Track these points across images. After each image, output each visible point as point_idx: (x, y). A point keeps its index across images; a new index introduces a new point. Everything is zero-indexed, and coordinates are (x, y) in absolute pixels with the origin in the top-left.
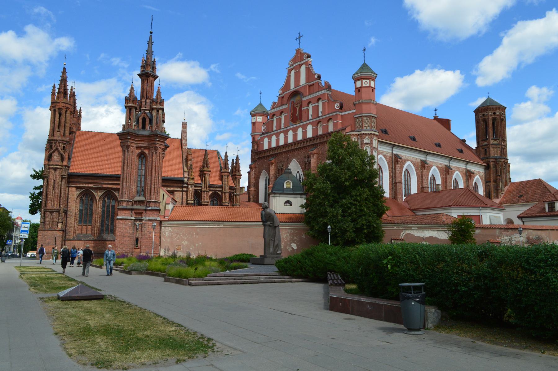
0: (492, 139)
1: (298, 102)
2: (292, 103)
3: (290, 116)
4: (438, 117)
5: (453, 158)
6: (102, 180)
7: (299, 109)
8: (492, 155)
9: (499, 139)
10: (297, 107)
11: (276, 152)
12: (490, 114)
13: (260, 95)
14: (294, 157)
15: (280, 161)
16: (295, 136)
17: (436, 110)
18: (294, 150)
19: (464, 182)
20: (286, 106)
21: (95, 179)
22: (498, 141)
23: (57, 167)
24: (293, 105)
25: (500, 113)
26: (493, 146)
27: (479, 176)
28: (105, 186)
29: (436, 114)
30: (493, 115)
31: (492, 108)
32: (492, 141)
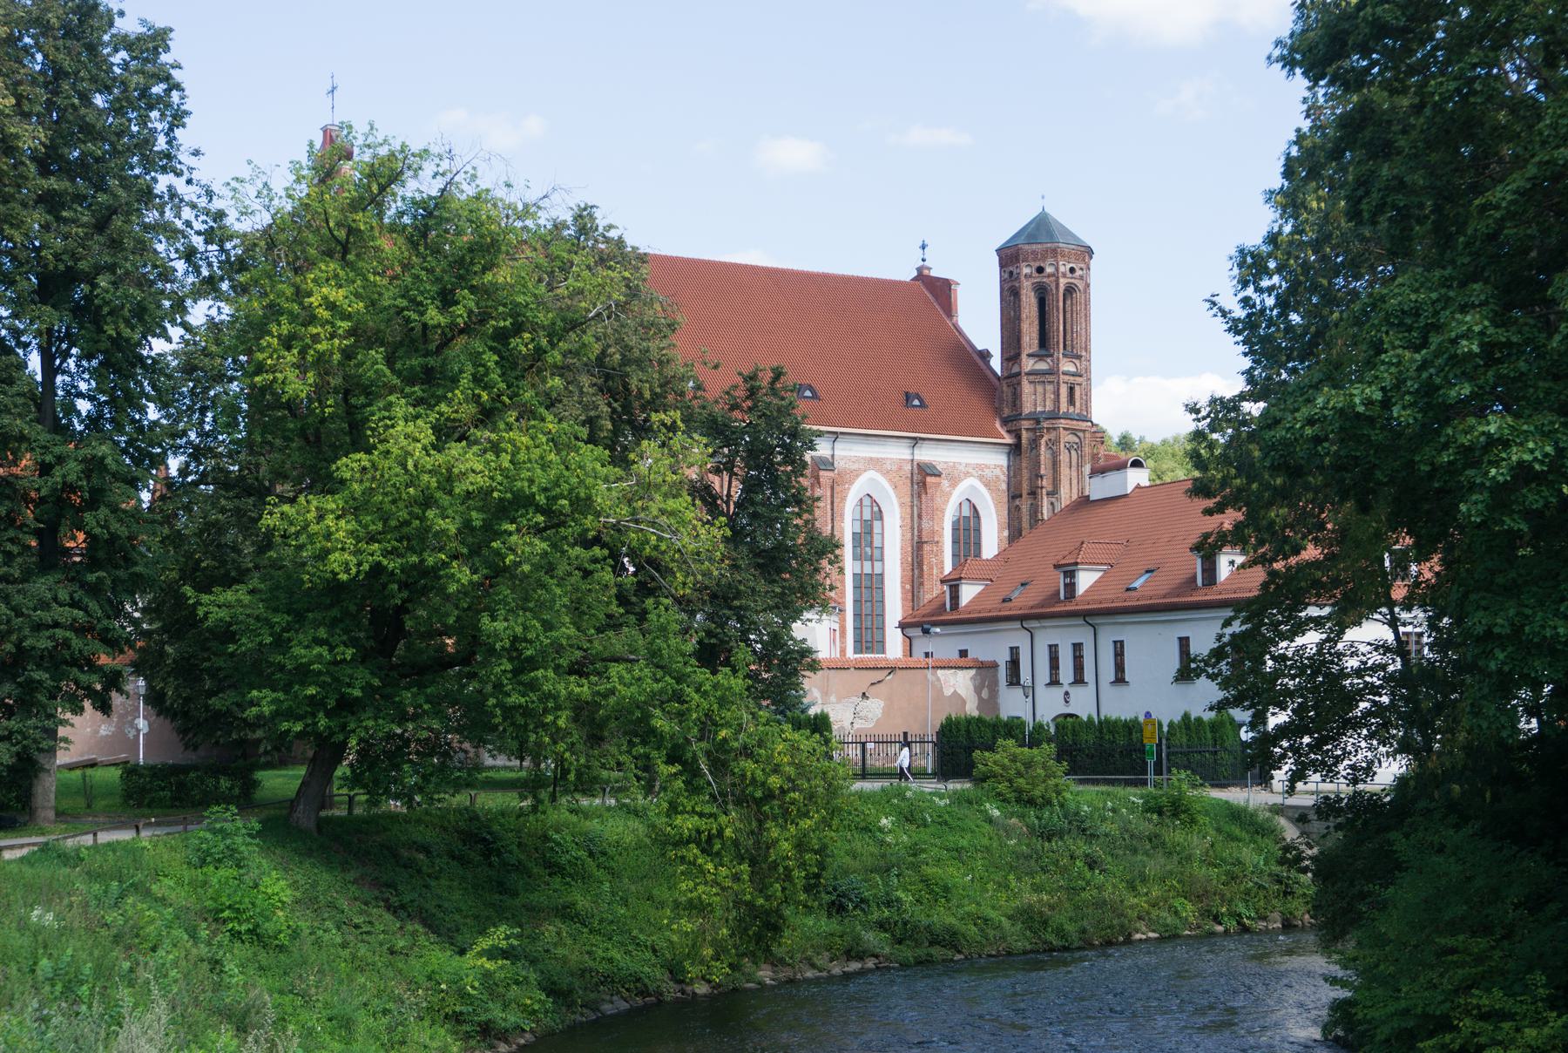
0: (1029, 355)
4: (929, 269)
5: (842, 433)
8: (1027, 408)
9: (1052, 356)
12: (1026, 270)
17: (923, 247)
19: (902, 505)
22: (1049, 360)
25: (1057, 269)
26: (1031, 378)
27: (981, 478)
29: (924, 260)
30: (1035, 274)
31: (1033, 252)
32: (1031, 361)
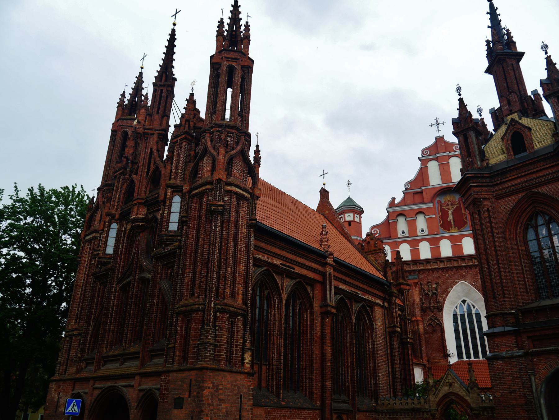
1: (450, 203)
2: (438, 203)
3: (438, 220)
6: (295, 253)
7: (453, 213)
10: (449, 209)
11: (415, 268)
13: (347, 187)
14: (464, 278)
15: (428, 282)
16: (457, 247)
18: (461, 268)
20: (430, 205)
21: (284, 249)
23: (244, 193)
24: (441, 206)
28: (298, 270)
